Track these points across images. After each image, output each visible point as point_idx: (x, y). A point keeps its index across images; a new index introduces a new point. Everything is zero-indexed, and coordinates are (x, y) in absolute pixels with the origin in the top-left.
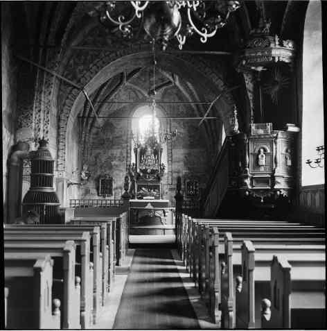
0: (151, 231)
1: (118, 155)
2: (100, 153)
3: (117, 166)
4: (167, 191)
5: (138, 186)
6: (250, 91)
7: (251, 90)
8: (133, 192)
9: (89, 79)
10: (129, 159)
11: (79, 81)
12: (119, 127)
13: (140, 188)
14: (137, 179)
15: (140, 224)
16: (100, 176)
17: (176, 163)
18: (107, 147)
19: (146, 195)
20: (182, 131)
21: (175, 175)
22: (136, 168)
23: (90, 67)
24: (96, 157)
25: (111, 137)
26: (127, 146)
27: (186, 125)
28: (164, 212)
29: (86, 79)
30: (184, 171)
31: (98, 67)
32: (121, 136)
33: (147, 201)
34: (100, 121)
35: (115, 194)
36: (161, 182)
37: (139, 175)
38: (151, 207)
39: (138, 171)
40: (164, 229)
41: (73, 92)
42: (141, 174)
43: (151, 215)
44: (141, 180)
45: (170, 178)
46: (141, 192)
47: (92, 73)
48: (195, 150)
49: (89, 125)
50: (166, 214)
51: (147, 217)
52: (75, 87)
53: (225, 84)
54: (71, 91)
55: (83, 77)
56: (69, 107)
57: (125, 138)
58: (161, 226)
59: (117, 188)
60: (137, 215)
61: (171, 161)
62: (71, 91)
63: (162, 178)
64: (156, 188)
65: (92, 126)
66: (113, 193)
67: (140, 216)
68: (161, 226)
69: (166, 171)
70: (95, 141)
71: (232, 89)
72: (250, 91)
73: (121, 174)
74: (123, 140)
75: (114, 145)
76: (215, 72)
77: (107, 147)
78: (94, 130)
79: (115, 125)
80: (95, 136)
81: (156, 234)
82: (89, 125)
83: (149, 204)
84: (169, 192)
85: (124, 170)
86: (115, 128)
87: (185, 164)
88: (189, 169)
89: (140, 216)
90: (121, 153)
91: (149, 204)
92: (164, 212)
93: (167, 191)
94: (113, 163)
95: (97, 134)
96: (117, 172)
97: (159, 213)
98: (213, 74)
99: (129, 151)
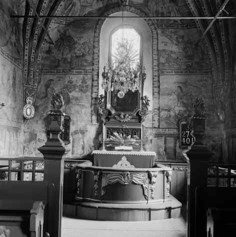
1: (80, 83)
2: (52, 80)
3: (77, 99)
4: (151, 137)
5: (108, 129)
8: (100, 139)
10: (95, 90)
12: (82, 41)
13: (110, 132)
14: (108, 119)
15: (103, 199)
17: (165, 97)
18: (63, 71)
19: (119, 144)
20: (175, 48)
21: (164, 114)
22: (105, 102)
24: (47, 86)
25: (69, 56)
26: (93, 70)
27: (180, 40)
28: (150, 177)
30: (178, 109)
32: (83, 55)
33: (120, 153)
34: (54, 29)
35: (73, 142)
36: (143, 123)
37: (110, 113)
38: (129, 167)
39: (109, 106)
40: (150, 210)
42: (113, 112)
43: (125, 181)
44: (112, 120)
45: (156, 118)
46: (112, 138)
48: (193, 77)
49: (36, 37)
50: (154, 179)
51: (118, 185)
57: (89, 58)
58: (142, 204)
59: (76, 132)
60: (100, 179)
61: (159, 93)
63: (144, 117)
64: (135, 132)
65: (40, 40)
66: (71, 139)
67: (104, 183)
68: (142, 204)
69: (150, 108)
70: (47, 62)
73: (83, 111)
74: (86, 61)
75: (73, 68)
77: (63, 71)
78: (44, 46)
79: (76, 39)
80: (45, 55)
81: (133, 220)
82: (36, 37)
83: (124, 159)
84: (155, 140)
85: (88, 105)
86: (75, 43)
87: (180, 98)
88: (184, 105)
89: (104, 183)
90: (84, 81)
91: (124, 159)
92: (150, 177)
93: (151, 137)
94: (70, 94)
95: (49, 52)
96: (77, 108)
97: (140, 179)
99: (95, 78)
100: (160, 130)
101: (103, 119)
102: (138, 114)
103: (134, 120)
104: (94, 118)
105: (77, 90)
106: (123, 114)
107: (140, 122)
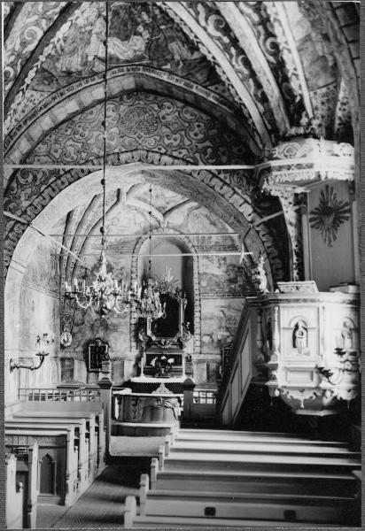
0: (158, 432)
6: (291, 224)
7: (294, 221)
9: (39, 207)
11: (25, 212)
16: (90, 341)
23: (42, 188)
27: (222, 262)
29: (36, 208)
31: (54, 190)
39: (149, 332)
41: (15, 229)
42: (154, 338)
47: (44, 199)
48: (236, 300)
52: (18, 222)
53: (255, 211)
54: (13, 227)
55: (31, 205)
56: (9, 251)
62: (13, 227)
71: (266, 219)
72: (291, 224)
73: (122, 337)
76: (239, 191)
83: (163, 386)
85: (127, 331)
91: (163, 386)
96: (115, 334)
98: (235, 196)
100: (202, 355)
101: (144, 346)
102: (179, 340)
103: (175, 347)
104: (134, 344)
105: (116, 316)
106: (163, 340)
107: (181, 348)
